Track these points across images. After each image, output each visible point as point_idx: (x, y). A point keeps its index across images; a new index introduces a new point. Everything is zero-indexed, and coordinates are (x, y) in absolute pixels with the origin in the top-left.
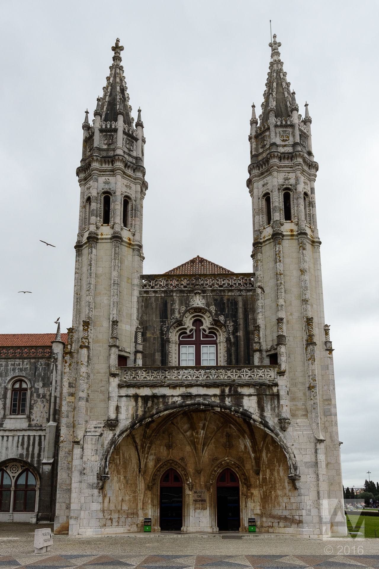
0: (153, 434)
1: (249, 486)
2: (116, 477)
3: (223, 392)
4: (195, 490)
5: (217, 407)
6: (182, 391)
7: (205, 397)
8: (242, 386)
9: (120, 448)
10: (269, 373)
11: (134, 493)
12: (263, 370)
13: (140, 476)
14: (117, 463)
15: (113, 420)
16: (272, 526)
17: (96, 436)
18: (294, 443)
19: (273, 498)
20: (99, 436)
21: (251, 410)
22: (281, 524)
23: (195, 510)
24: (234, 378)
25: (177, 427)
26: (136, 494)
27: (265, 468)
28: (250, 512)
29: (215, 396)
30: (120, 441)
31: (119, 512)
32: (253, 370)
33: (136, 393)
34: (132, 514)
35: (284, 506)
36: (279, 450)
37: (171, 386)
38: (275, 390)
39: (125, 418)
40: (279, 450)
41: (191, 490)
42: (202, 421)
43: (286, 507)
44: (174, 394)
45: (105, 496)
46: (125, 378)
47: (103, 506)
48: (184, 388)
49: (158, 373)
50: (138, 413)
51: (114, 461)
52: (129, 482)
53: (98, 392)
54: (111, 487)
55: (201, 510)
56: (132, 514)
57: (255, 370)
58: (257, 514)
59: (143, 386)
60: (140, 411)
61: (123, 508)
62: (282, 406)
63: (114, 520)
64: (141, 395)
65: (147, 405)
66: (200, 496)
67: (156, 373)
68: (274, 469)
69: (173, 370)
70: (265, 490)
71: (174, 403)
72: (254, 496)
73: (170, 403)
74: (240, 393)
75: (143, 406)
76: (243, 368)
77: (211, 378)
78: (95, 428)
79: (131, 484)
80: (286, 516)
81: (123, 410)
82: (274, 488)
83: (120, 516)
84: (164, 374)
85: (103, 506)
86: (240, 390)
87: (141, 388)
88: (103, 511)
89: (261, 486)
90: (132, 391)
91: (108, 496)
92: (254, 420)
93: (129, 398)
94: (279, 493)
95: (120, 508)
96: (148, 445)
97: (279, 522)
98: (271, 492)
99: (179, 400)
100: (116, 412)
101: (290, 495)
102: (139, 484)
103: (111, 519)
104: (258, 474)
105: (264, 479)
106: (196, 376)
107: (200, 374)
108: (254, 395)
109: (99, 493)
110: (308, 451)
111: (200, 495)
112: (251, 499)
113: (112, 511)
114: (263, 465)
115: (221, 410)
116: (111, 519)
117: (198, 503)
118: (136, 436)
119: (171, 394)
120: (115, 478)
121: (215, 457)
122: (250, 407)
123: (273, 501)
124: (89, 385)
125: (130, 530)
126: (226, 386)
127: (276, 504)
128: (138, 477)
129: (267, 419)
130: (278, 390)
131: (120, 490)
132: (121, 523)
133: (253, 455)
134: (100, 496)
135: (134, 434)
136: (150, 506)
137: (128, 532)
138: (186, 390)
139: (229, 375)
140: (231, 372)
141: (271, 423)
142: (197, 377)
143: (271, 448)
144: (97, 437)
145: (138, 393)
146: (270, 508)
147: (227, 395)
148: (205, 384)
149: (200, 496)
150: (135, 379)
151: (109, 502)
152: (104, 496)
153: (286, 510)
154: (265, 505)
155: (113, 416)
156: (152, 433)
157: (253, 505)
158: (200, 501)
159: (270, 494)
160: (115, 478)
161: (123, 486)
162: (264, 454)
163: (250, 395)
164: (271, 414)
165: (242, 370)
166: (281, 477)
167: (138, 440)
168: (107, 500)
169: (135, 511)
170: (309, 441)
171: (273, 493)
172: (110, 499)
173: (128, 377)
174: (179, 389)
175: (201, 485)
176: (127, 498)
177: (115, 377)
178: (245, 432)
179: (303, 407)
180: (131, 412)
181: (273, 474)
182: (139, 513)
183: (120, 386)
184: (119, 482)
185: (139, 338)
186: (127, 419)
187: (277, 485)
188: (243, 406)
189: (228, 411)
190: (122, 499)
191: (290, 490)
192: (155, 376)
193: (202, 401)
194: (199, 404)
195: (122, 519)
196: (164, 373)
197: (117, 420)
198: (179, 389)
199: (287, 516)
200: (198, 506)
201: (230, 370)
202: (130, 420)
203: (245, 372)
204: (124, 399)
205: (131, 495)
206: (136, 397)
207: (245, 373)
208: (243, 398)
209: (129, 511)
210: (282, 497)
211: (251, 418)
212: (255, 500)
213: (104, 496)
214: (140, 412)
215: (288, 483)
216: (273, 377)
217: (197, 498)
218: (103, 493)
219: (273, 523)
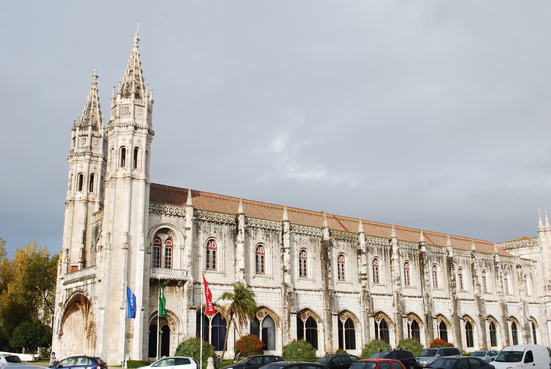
26: (83, 341)
31: (70, 351)
51: (68, 324)
52: (78, 335)
61: (73, 349)
88: (61, 350)
91: (64, 342)
120: (69, 333)
136: (87, 348)
152: (62, 343)
155: (61, 302)
168: (63, 345)
173: (65, 280)
176: (76, 343)
197: (62, 303)
206: (66, 289)
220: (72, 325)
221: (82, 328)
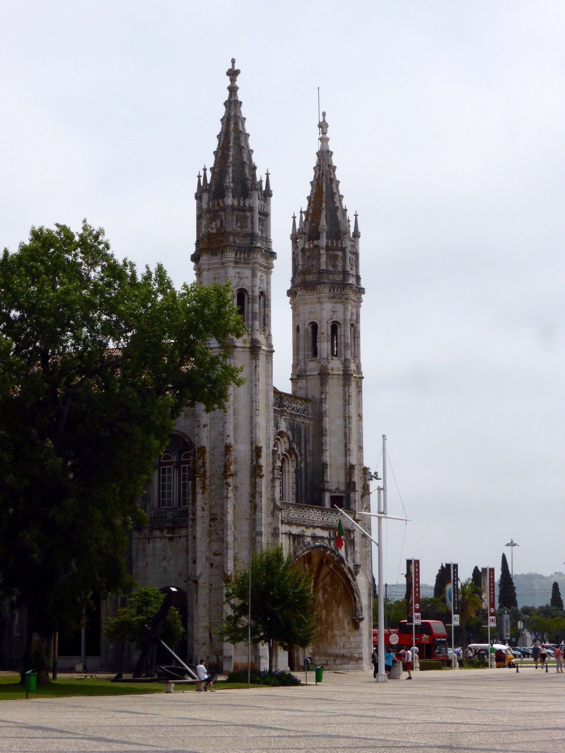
16: (326, 663)
19: (329, 638)
35: (343, 645)
36: (339, 592)
40: (339, 592)
43: (344, 646)
68: (332, 610)
82: (331, 628)
94: (337, 632)
97: (335, 660)
98: (326, 632)
114: (318, 605)
143: (329, 589)
146: (325, 647)
166: (339, 618)
171: (329, 632)
181: (330, 615)
187: (335, 626)
191: (349, 631)
210: (340, 636)
215: (348, 624)
219: (327, 661)
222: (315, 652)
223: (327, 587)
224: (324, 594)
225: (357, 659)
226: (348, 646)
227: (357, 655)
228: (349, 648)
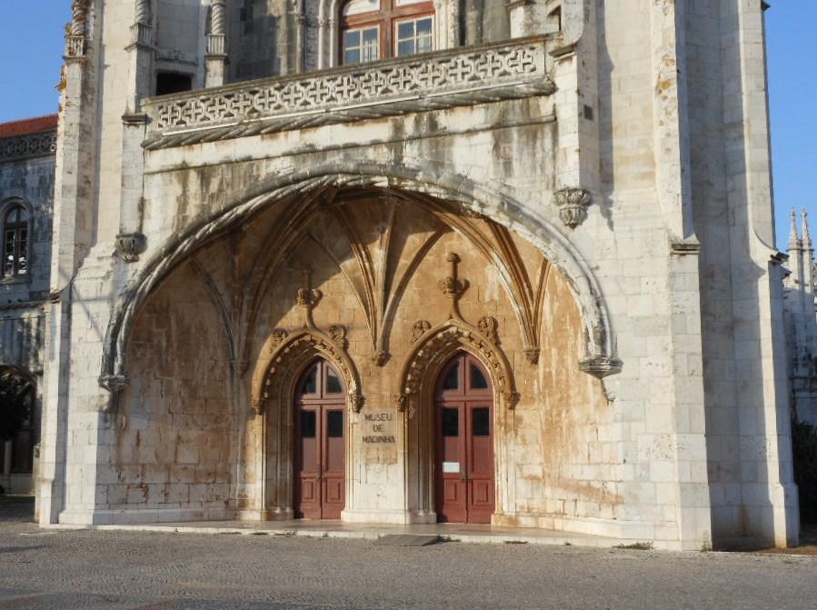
0: (255, 269)
1: (514, 399)
2: (158, 381)
3: (398, 128)
4: (366, 412)
5: (380, 175)
6: (293, 140)
7: (350, 152)
8: (451, 106)
9: (168, 307)
10: (529, 60)
11: (216, 421)
12: (512, 55)
13: (235, 380)
14: (159, 345)
15: (128, 236)
17: (97, 278)
18: (599, 263)
19: (564, 429)
20: (104, 278)
21: (475, 175)
22: (582, 508)
23: (366, 465)
24: (429, 89)
25: (321, 245)
26: (224, 425)
27: (549, 344)
28: (511, 470)
29: (375, 144)
30: (147, 289)
31: (168, 468)
32: (482, 56)
33: (184, 162)
34: (209, 474)
35: (587, 455)
37: (263, 132)
38: (545, 106)
39: (157, 228)
41: (358, 412)
42: (377, 222)
43: (589, 455)
44: (272, 153)
45: (124, 429)
46: (160, 126)
47: (119, 455)
48: (297, 133)
49: (235, 102)
50: (188, 213)
51: (149, 340)
52: (201, 393)
53: (111, 170)
54: (142, 406)
55: (383, 464)
56: (209, 474)
57: (489, 57)
58: (533, 478)
59: (197, 141)
60: (192, 206)
61: (180, 460)
62: (565, 153)
63: (152, 488)
64: (192, 165)
65: (207, 191)
66: (379, 428)
67: (228, 102)
69: (272, 89)
70: (548, 408)
71: (272, 176)
72: (525, 427)
73: (263, 174)
74: (445, 128)
75: (199, 192)
76: (454, 55)
77: (367, 96)
78: (100, 259)
79: (206, 400)
80: (589, 481)
81: (153, 209)
82: (565, 401)
83: (172, 480)
84: (249, 103)
85: (119, 455)
86: (444, 119)
87: (194, 146)
89: (541, 397)
90: (175, 156)
92: (482, 205)
93: (167, 176)
94: (576, 414)
95: (173, 459)
96: (247, 297)
97: (576, 501)
98: (559, 414)
99: (283, 167)
100: (137, 215)
101: (598, 421)
102: (233, 398)
103: (144, 488)
104: (535, 361)
105: (548, 376)
106: (328, 97)
107: (337, 89)
108: (484, 130)
109: (106, 421)
110: (644, 285)
111: (377, 423)
112: (516, 434)
113: (147, 467)
115: (390, 181)
116: (144, 488)
117: (376, 445)
118: (215, 277)
119: (262, 155)
121: (418, 319)
122: (471, 166)
123: (564, 441)
124: (89, 154)
125: (202, 515)
126: (407, 113)
127: (570, 447)
128: (228, 382)
129: (520, 197)
130: (555, 105)
131: (170, 412)
132: (173, 496)
133: (516, 309)
134: (106, 429)
135: (208, 270)
137: (195, 518)
138: (301, 140)
139: (415, 81)
140: (422, 73)
141: (530, 207)
142: (332, 99)
144: (101, 281)
145: (188, 161)
146: (559, 460)
147: (411, 139)
148: (348, 115)
149: (379, 428)
150: (183, 125)
151: (138, 444)
153: (590, 464)
154: (550, 452)
155: (132, 228)
156: (254, 265)
157: (520, 450)
158: (380, 439)
159: (558, 418)
160: (155, 384)
161: (180, 404)
162: (546, 307)
163: (470, 132)
164: (533, 182)
165: (453, 60)
167: (221, 287)
168: (129, 440)
169: (220, 466)
170: (650, 252)
171: (563, 415)
172: (138, 435)
174: (286, 136)
175: (381, 397)
177: (136, 125)
178: (490, 245)
179: (642, 151)
180: (172, 210)
182: (232, 472)
183: (149, 147)
184: (167, 395)
185: (216, 22)
186: (163, 229)
187: (572, 392)
188: (452, 166)
189: (410, 183)
190: (179, 437)
192: (229, 110)
193: (338, 162)
194: (329, 172)
195: (179, 488)
196: (248, 100)
198: (286, 136)
199: (592, 484)
200: (374, 453)
201: (420, 66)
202: (169, 233)
203: (460, 66)
204: (158, 177)
205: (206, 425)
206: (183, 168)
207: (460, 70)
208: (451, 144)
209: (201, 467)
211: (473, 198)
212: (527, 437)
213: (121, 430)
214: (192, 212)
216: (540, 71)
217: (373, 434)
218: (119, 421)
220: (169, 346)
221: (221, 364)
222: (544, 472)
223: (557, 278)
224: (552, 302)
225: (614, 500)
226: (595, 459)
227: (611, 487)
228: (599, 464)
